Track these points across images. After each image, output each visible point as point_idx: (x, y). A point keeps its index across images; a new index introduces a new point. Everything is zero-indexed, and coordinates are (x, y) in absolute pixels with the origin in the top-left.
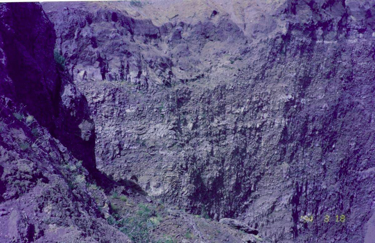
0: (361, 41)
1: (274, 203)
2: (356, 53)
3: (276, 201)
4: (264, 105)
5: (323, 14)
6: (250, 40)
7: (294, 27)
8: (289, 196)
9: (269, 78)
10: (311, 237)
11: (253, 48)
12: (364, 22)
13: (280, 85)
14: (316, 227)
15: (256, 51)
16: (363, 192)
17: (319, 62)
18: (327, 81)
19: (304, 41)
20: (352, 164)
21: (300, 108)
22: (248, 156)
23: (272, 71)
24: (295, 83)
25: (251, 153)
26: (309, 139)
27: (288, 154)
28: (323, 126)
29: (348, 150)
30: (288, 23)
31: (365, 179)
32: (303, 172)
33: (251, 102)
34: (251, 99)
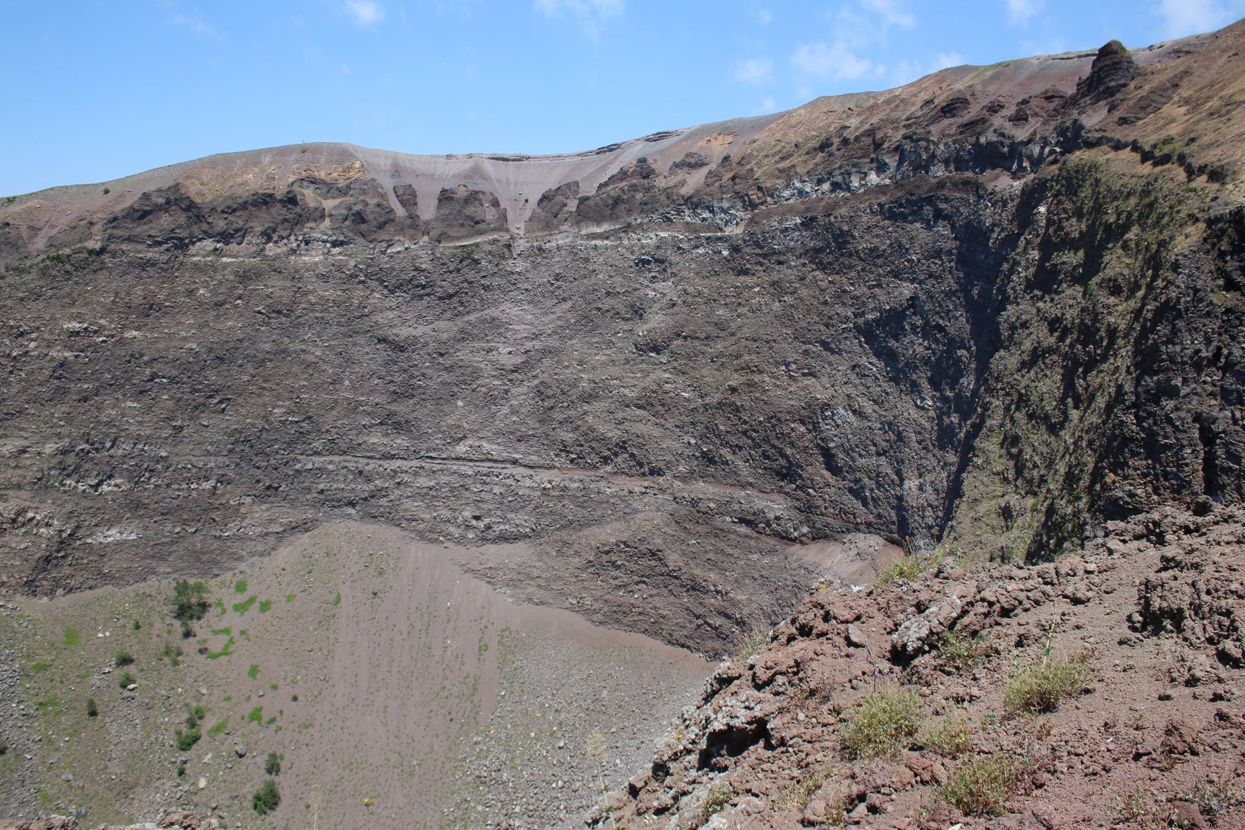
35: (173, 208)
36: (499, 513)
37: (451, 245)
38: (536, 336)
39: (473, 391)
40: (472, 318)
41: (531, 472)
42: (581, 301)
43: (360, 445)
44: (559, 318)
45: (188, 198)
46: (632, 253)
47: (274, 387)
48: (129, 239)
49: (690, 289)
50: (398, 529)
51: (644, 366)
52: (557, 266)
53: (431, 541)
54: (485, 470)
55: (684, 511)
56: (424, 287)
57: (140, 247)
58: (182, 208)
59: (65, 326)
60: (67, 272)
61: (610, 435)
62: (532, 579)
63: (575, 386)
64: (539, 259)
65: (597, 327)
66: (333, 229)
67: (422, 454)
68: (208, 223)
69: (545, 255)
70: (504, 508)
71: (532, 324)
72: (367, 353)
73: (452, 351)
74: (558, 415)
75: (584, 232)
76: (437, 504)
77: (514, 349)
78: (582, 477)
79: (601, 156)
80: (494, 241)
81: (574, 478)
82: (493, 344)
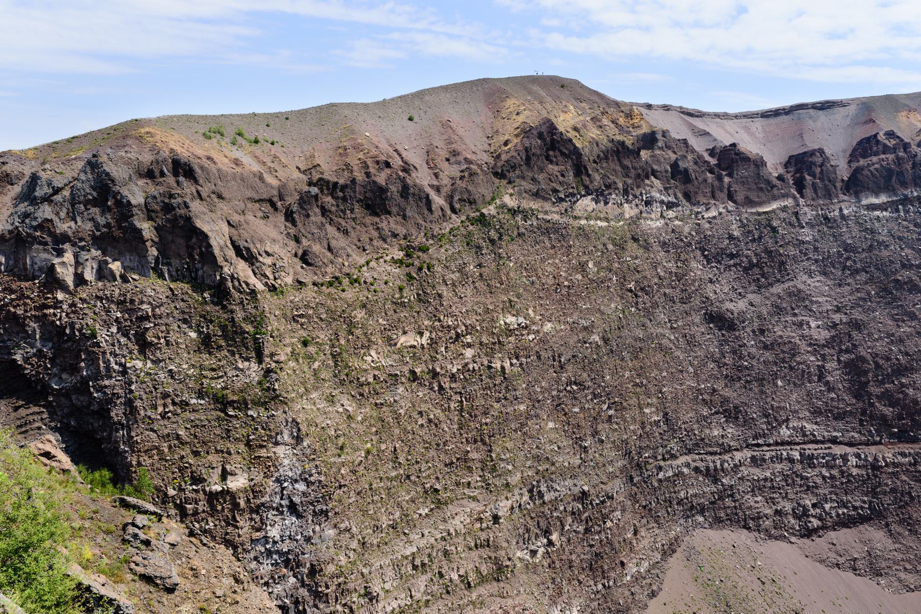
35: (551, 153)
36: (834, 497)
37: (754, 210)
38: (838, 310)
39: (791, 368)
40: (778, 289)
41: (855, 450)
42: (877, 274)
43: (702, 440)
44: (858, 290)
45: (570, 140)
46: (916, 225)
47: (645, 382)
48: (536, 195)
50: (745, 530)
53: (776, 538)
54: (815, 452)
56: (732, 256)
57: (547, 206)
58: (563, 154)
59: (502, 322)
60: (492, 242)
62: (898, 565)
63: (888, 359)
64: (826, 229)
65: (895, 299)
66: (666, 189)
67: (751, 441)
68: (589, 176)
70: (838, 491)
71: (829, 296)
72: (703, 333)
73: (770, 327)
74: (875, 390)
75: (865, 202)
76: (774, 495)
77: (820, 323)
78: (912, 451)
79: (772, 121)
80: (784, 209)
82: (804, 318)
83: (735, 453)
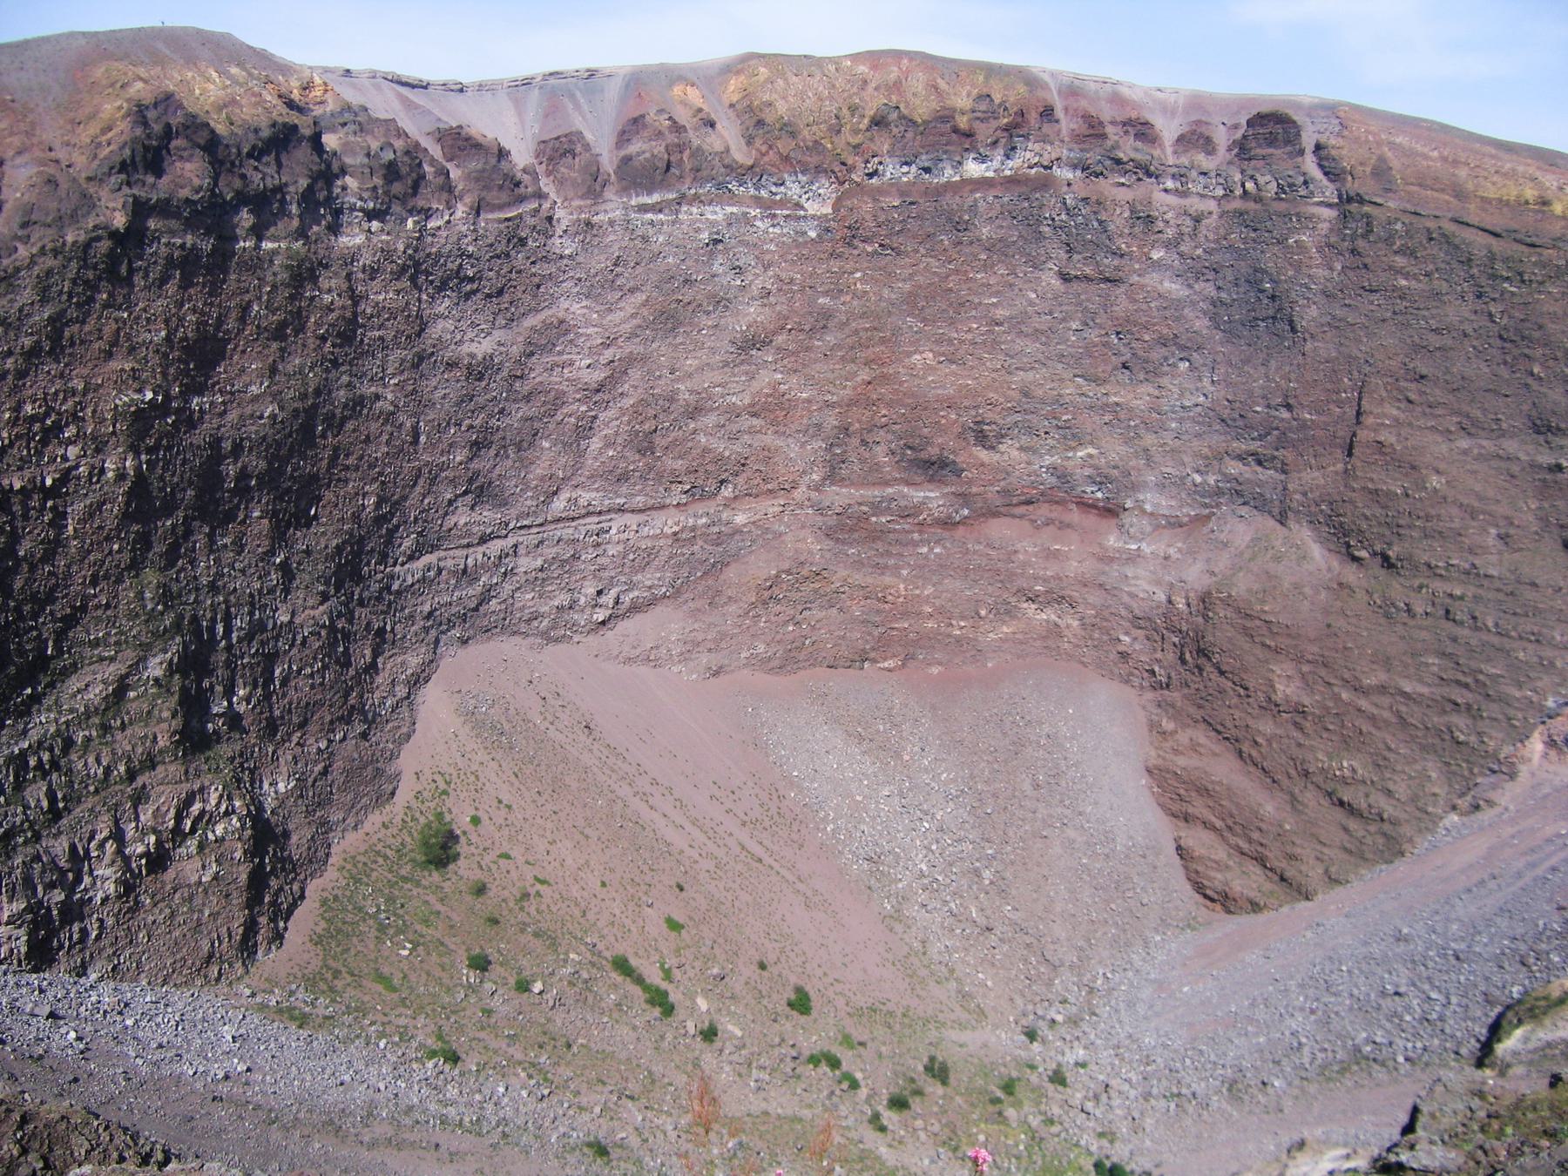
0: (375, 239)
1: (123, 678)
2: (364, 271)
3: (127, 675)
4: (67, 425)
5: (249, 172)
6: (8, 248)
7: (154, 207)
8: (169, 655)
9: (78, 350)
10: (254, 746)
11: (18, 270)
12: (380, 191)
13: (115, 365)
14: (266, 719)
15: (27, 280)
16: (411, 617)
17: (247, 297)
18: (275, 345)
19: (188, 245)
20: (373, 550)
21: (190, 421)
22: (25, 567)
23: (87, 328)
24: (166, 355)
25: (32, 556)
26: (230, 502)
27: (159, 548)
28: (270, 463)
29: (356, 517)
30: (131, 200)
31: (413, 585)
32: (213, 588)
33: (17, 418)
34: (17, 408)
40: (531, 321)
44: (633, 316)
49: (783, 275)
51: (745, 367)
52: (616, 247)
53: (557, 640)
55: (833, 520)
61: (727, 454)
63: (672, 399)
69: (595, 232)
71: (601, 326)
75: (633, 203)
76: (550, 588)
81: (699, 516)
83: (496, 541)
